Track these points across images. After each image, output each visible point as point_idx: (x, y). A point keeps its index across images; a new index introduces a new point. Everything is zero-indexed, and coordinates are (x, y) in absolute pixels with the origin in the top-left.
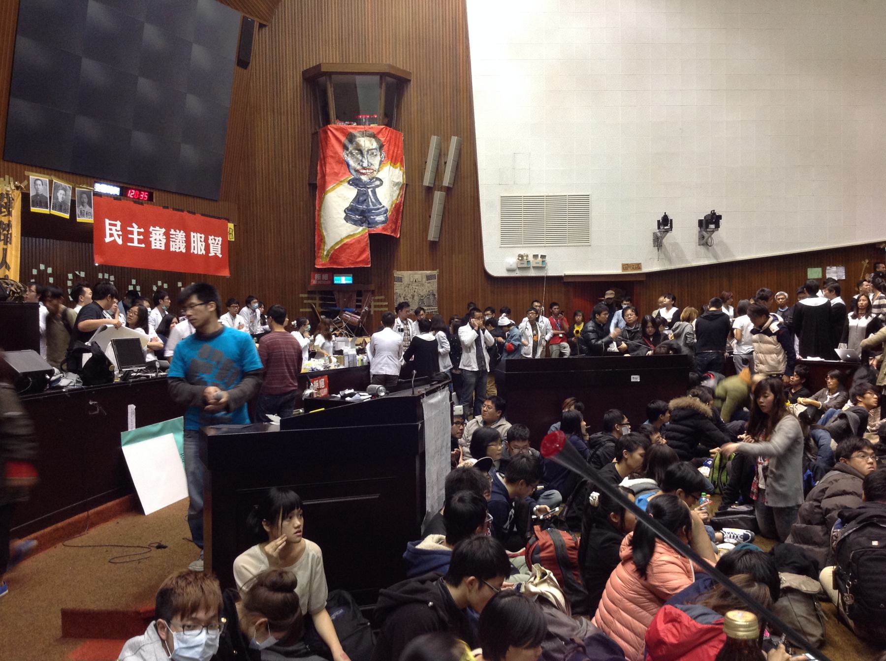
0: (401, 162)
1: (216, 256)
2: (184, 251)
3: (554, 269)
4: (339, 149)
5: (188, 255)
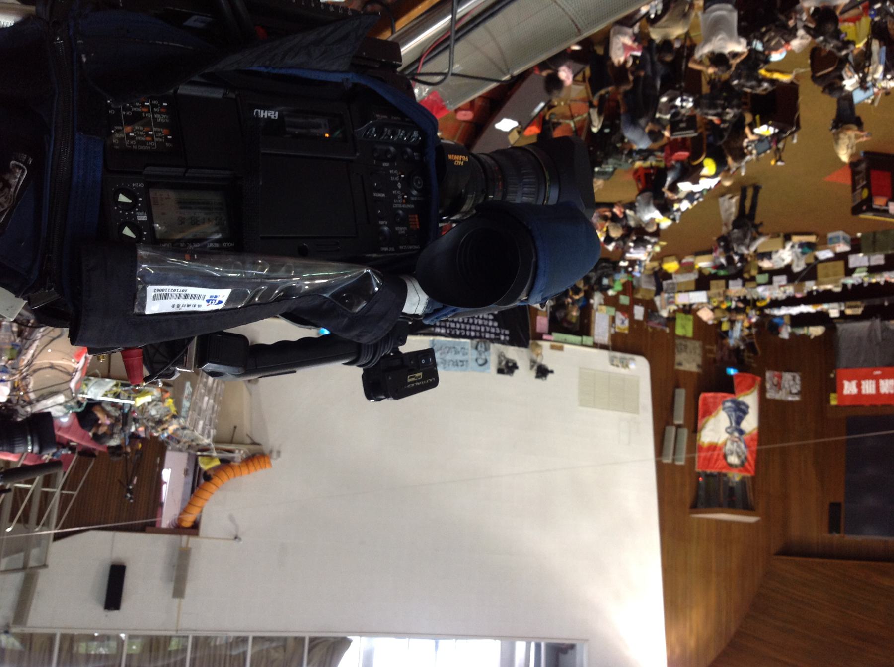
0: (701, 448)
1: (850, 380)
2: (882, 382)
3: (605, 354)
4: (750, 458)
5: (877, 379)
